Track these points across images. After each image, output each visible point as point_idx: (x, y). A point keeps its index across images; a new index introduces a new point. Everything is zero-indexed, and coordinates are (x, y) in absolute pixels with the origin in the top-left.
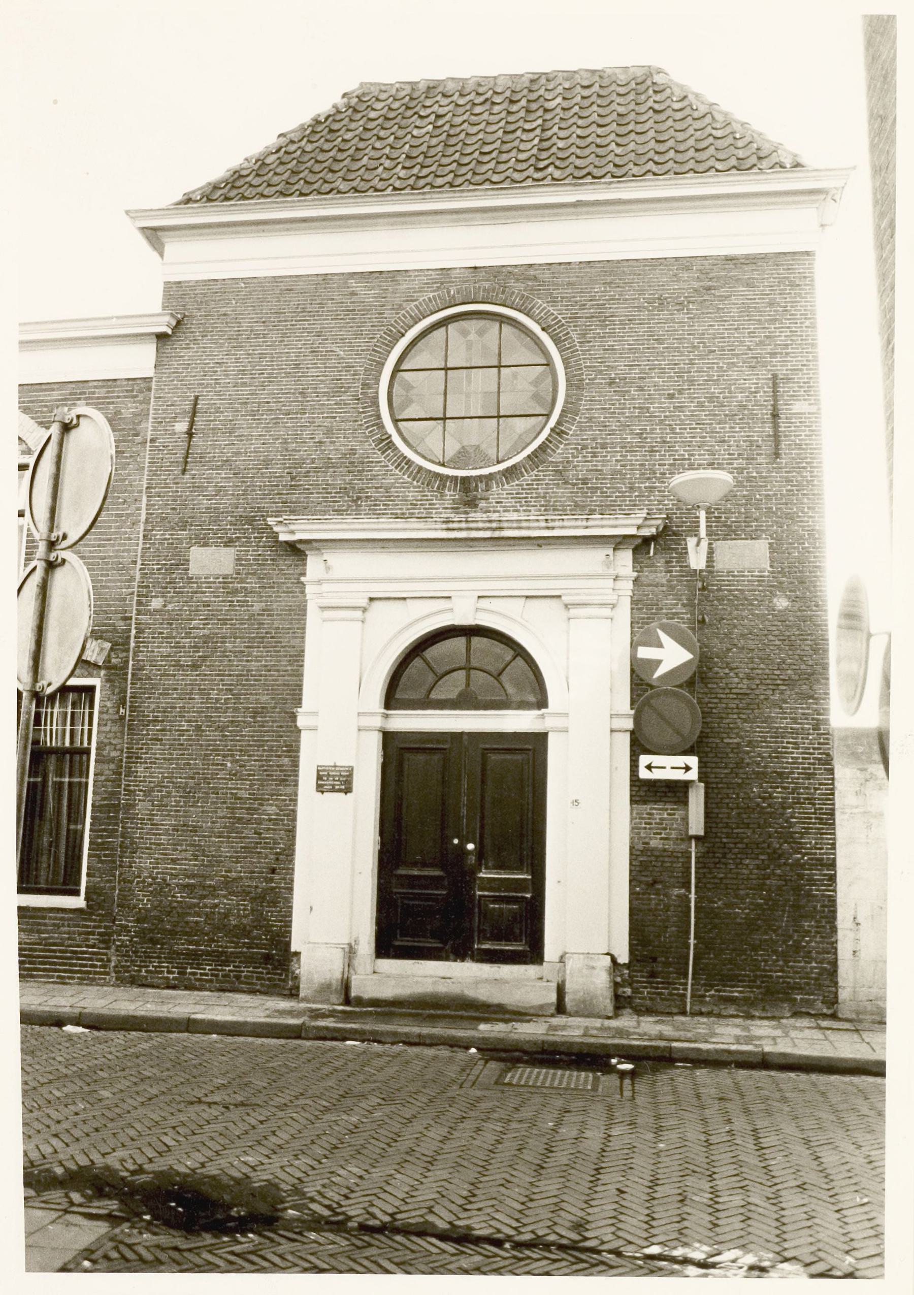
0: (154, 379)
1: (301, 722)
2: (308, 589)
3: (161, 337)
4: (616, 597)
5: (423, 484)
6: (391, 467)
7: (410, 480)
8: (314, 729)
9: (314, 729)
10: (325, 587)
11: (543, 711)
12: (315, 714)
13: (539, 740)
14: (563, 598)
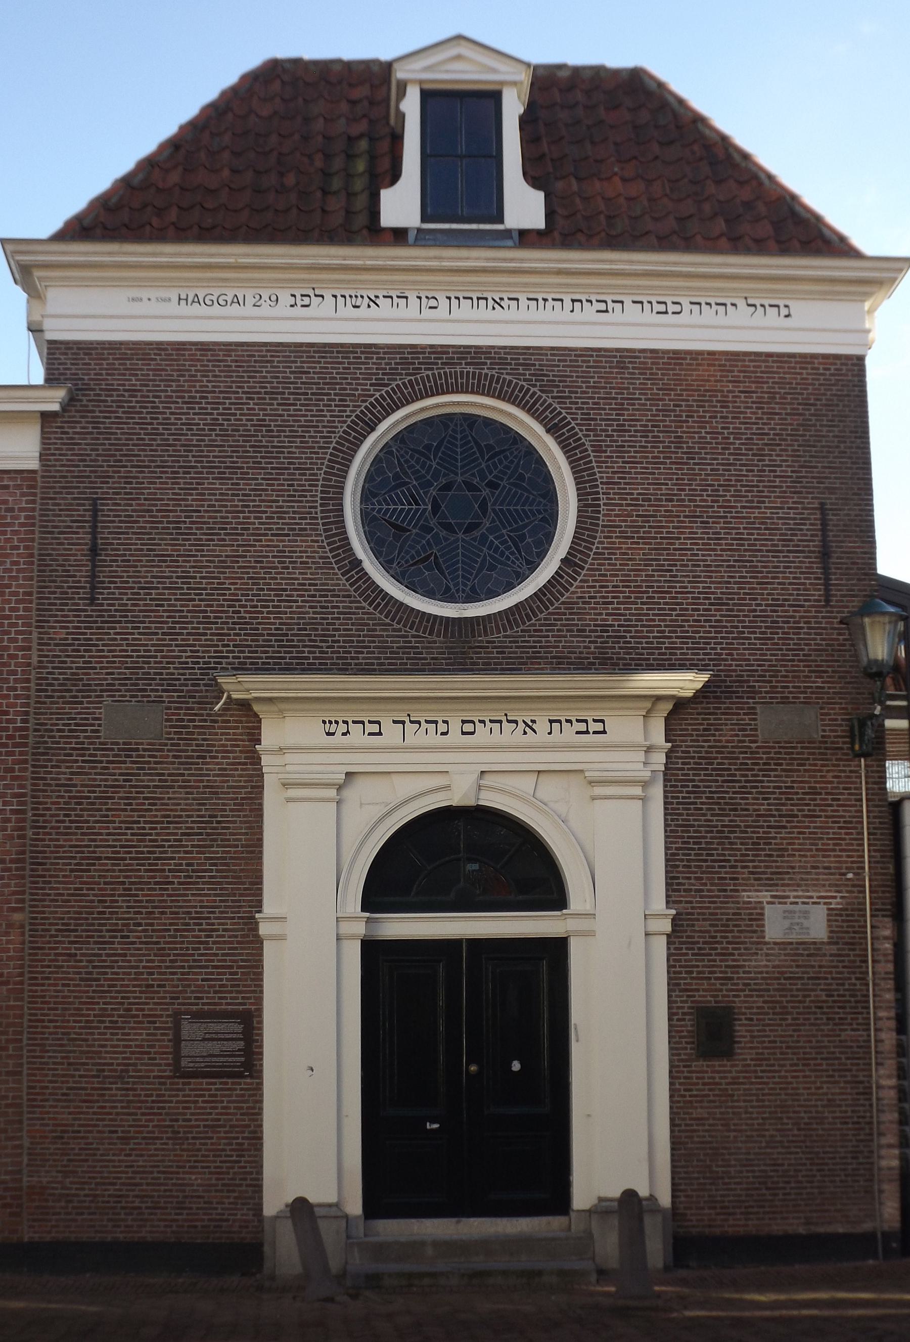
0: (40, 473)
1: (264, 929)
2: (265, 760)
3: (46, 417)
4: (649, 774)
5: (405, 626)
6: (364, 604)
7: (388, 621)
8: (281, 938)
9: (281, 938)
10: (289, 758)
11: (564, 911)
12: (282, 919)
13: (557, 949)
14: (587, 774)
